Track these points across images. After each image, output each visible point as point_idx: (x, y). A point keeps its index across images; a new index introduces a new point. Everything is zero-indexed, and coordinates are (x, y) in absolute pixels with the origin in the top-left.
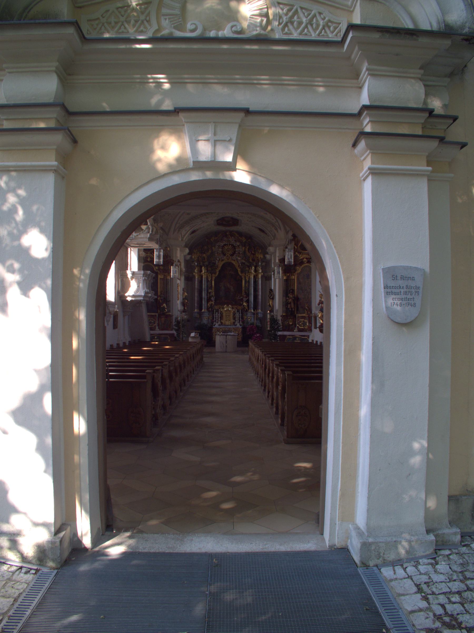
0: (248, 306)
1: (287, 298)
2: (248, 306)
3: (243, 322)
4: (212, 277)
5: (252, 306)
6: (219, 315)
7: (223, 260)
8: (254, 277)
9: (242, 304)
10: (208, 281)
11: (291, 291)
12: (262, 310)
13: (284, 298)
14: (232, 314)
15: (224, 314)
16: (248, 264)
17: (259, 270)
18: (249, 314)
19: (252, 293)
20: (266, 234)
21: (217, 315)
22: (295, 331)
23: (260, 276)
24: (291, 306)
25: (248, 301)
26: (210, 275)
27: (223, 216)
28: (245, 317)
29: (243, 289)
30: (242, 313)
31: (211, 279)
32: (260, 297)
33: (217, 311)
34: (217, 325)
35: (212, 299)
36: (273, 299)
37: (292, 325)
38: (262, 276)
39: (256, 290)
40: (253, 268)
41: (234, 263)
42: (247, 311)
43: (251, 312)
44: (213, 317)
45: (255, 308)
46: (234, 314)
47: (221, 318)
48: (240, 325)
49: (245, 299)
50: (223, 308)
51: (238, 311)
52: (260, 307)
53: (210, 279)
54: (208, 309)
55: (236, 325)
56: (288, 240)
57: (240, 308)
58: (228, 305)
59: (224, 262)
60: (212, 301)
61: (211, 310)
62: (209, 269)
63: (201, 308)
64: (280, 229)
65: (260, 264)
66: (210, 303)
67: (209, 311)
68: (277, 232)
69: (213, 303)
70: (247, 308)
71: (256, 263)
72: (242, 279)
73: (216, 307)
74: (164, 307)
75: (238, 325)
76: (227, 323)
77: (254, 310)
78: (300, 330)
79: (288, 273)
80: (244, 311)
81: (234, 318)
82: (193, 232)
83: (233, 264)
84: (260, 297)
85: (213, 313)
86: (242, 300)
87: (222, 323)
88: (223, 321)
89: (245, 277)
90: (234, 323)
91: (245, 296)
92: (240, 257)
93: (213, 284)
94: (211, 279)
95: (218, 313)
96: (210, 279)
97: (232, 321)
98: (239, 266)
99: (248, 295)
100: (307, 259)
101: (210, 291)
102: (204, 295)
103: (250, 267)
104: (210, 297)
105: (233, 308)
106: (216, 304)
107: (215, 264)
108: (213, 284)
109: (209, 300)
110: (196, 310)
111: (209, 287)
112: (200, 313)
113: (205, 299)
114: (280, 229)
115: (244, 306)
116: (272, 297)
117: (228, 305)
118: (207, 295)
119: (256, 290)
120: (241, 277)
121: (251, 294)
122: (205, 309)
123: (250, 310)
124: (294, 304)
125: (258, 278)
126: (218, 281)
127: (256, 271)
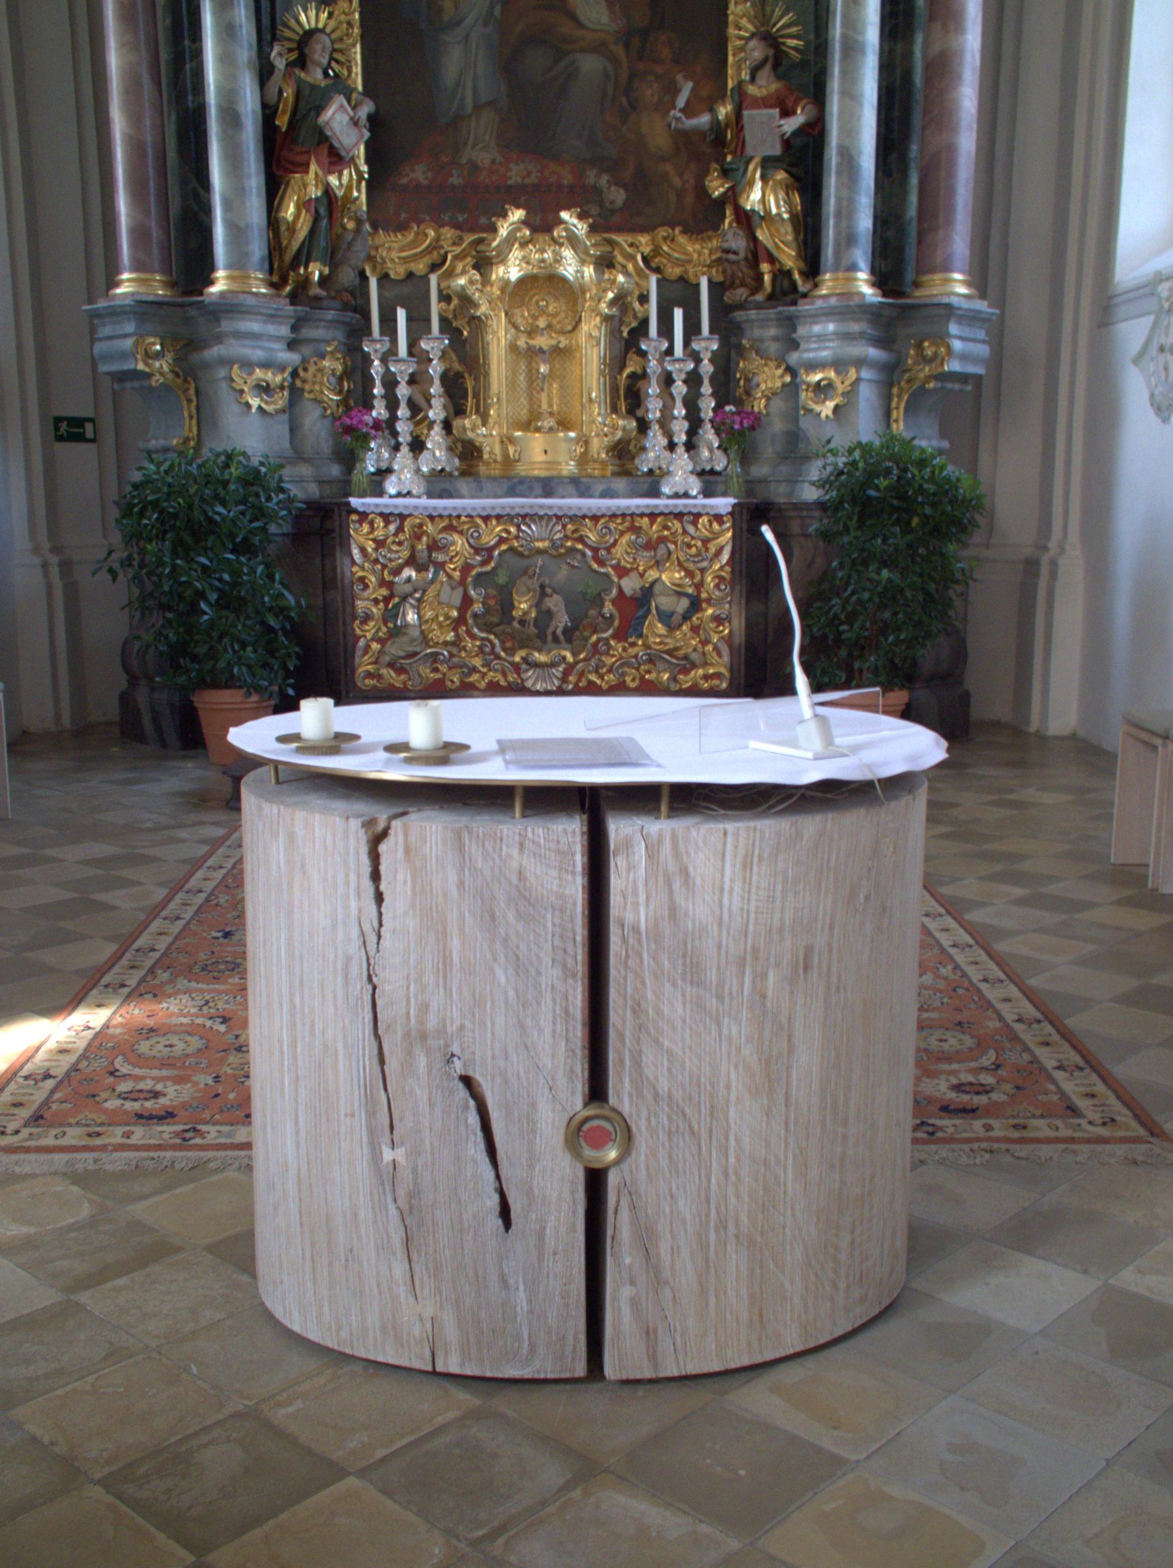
0: (808, 227)
2: (808, 227)
3: (740, 437)
5: (865, 222)
6: (434, 344)
9: (733, 196)
12: (980, 282)
14: (591, 343)
15: (499, 339)
18: (822, 337)
19: (872, 35)
21: (397, 352)
25: (803, 162)
28: (770, 378)
30: (726, 323)
32: (967, 97)
33: (410, 292)
34: (403, 483)
35: (341, 120)
42: (786, 292)
43: (850, 308)
44: (356, 370)
45: (898, 259)
46: (627, 340)
47: (462, 390)
48: (710, 481)
49: (769, 129)
50: (483, 264)
51: (680, 292)
52: (959, 240)
54: (282, 266)
55: (652, 484)
57: (694, 256)
58: (542, 225)
60: (336, 159)
61: (317, 279)
63: (193, 265)
66: (311, 182)
69: (349, 182)
70: (789, 257)
73: (396, 251)
75: (681, 474)
76: (538, 452)
77: (884, 279)
80: (758, 293)
81: (629, 397)
84: (967, 97)
85: (358, 331)
86: (721, 147)
87: (468, 453)
88: (486, 434)
90: (624, 453)
91: (766, 86)
95: (419, 324)
97: (602, 425)
99: (804, 75)
104: (310, 104)
105: (605, 263)
109: (286, 145)
110: (127, 286)
112: (185, 310)
113: (231, 118)
115: (746, 220)
117: (542, 225)
118: (264, 72)
121: (852, 48)
122: (238, 264)
123: (828, 282)
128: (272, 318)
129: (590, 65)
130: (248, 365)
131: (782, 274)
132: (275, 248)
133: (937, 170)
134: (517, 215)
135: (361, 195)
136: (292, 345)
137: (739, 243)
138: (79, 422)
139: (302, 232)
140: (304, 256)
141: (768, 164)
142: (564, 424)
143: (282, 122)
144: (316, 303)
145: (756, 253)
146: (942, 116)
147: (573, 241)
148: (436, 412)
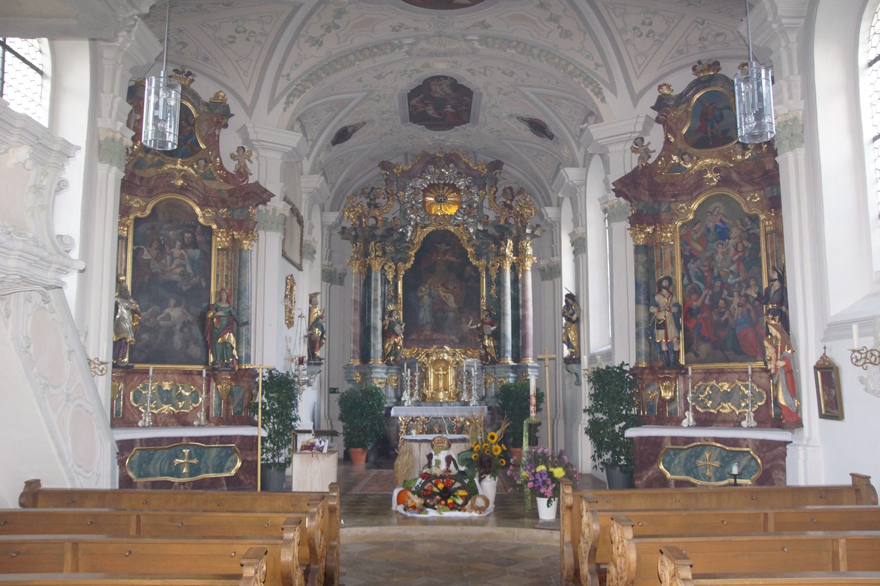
1: (653, 309)
4: (396, 271)
7: (426, 226)
8: (514, 268)
10: (385, 281)
11: (665, 283)
13: (642, 307)
16: (497, 234)
17: (526, 250)
20: (551, 137)
22: (685, 423)
23: (529, 264)
24: (666, 338)
25: (497, 336)
26: (392, 264)
27: (428, 73)
29: (483, 301)
31: (396, 277)
35: (397, 328)
36: (578, 321)
37: (673, 399)
38: (533, 264)
39: (517, 305)
40: (510, 242)
41: (458, 234)
52: (530, 351)
53: (390, 277)
54: (385, 357)
56: (642, 120)
59: (430, 229)
60: (397, 336)
62: (390, 249)
64: (614, 91)
65: (528, 231)
67: (388, 364)
68: (603, 100)
69: (399, 340)
70: (494, 355)
71: (518, 231)
72: (479, 274)
74: (226, 343)
77: (514, 360)
78: (703, 421)
79: (649, 225)
82: (342, 136)
83: (452, 235)
84: (530, 323)
87: (424, 397)
89: (487, 270)
90: (458, 395)
91: (488, 320)
92: (474, 217)
93: (400, 291)
94: (396, 277)
96: (390, 277)
98: (470, 240)
99: (497, 318)
100: (717, 170)
101: (391, 307)
102: (377, 321)
103: (499, 241)
106: (407, 343)
107: (404, 235)
108: (400, 291)
109: (388, 333)
111: (390, 297)
114: (614, 91)
115: (485, 347)
116: (574, 317)
119: (517, 305)
120: (476, 268)
124: (678, 328)
125: (524, 272)
126: (413, 281)
127: (517, 251)
128: (383, 368)
129: (451, 315)
130: (378, 378)
131: (492, 358)
132: (383, 353)
133: (525, 337)
134: (435, 347)
135: (401, 342)
136: (386, 374)
137: (483, 352)
138: (335, 389)
139: (389, 350)
140: (389, 355)
141: (489, 336)
142: (445, 390)
143: (386, 328)
144: (391, 365)
145: (487, 354)
146: (525, 327)
147: (447, 352)
148: (417, 388)
